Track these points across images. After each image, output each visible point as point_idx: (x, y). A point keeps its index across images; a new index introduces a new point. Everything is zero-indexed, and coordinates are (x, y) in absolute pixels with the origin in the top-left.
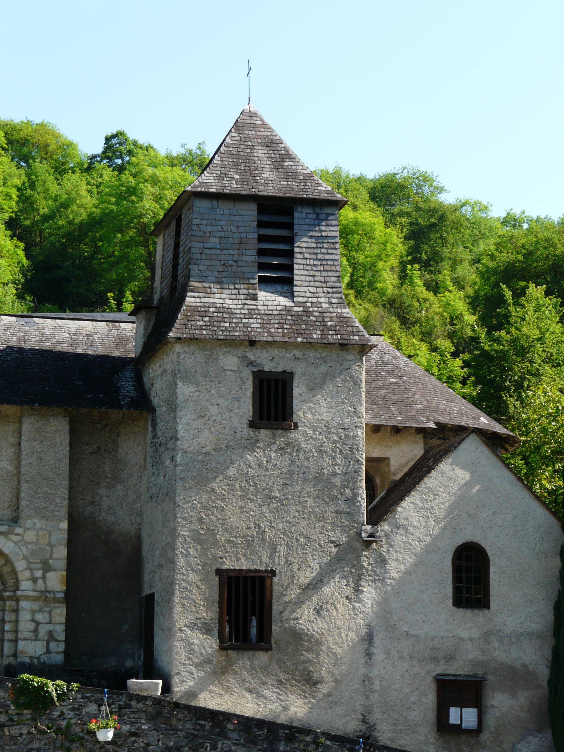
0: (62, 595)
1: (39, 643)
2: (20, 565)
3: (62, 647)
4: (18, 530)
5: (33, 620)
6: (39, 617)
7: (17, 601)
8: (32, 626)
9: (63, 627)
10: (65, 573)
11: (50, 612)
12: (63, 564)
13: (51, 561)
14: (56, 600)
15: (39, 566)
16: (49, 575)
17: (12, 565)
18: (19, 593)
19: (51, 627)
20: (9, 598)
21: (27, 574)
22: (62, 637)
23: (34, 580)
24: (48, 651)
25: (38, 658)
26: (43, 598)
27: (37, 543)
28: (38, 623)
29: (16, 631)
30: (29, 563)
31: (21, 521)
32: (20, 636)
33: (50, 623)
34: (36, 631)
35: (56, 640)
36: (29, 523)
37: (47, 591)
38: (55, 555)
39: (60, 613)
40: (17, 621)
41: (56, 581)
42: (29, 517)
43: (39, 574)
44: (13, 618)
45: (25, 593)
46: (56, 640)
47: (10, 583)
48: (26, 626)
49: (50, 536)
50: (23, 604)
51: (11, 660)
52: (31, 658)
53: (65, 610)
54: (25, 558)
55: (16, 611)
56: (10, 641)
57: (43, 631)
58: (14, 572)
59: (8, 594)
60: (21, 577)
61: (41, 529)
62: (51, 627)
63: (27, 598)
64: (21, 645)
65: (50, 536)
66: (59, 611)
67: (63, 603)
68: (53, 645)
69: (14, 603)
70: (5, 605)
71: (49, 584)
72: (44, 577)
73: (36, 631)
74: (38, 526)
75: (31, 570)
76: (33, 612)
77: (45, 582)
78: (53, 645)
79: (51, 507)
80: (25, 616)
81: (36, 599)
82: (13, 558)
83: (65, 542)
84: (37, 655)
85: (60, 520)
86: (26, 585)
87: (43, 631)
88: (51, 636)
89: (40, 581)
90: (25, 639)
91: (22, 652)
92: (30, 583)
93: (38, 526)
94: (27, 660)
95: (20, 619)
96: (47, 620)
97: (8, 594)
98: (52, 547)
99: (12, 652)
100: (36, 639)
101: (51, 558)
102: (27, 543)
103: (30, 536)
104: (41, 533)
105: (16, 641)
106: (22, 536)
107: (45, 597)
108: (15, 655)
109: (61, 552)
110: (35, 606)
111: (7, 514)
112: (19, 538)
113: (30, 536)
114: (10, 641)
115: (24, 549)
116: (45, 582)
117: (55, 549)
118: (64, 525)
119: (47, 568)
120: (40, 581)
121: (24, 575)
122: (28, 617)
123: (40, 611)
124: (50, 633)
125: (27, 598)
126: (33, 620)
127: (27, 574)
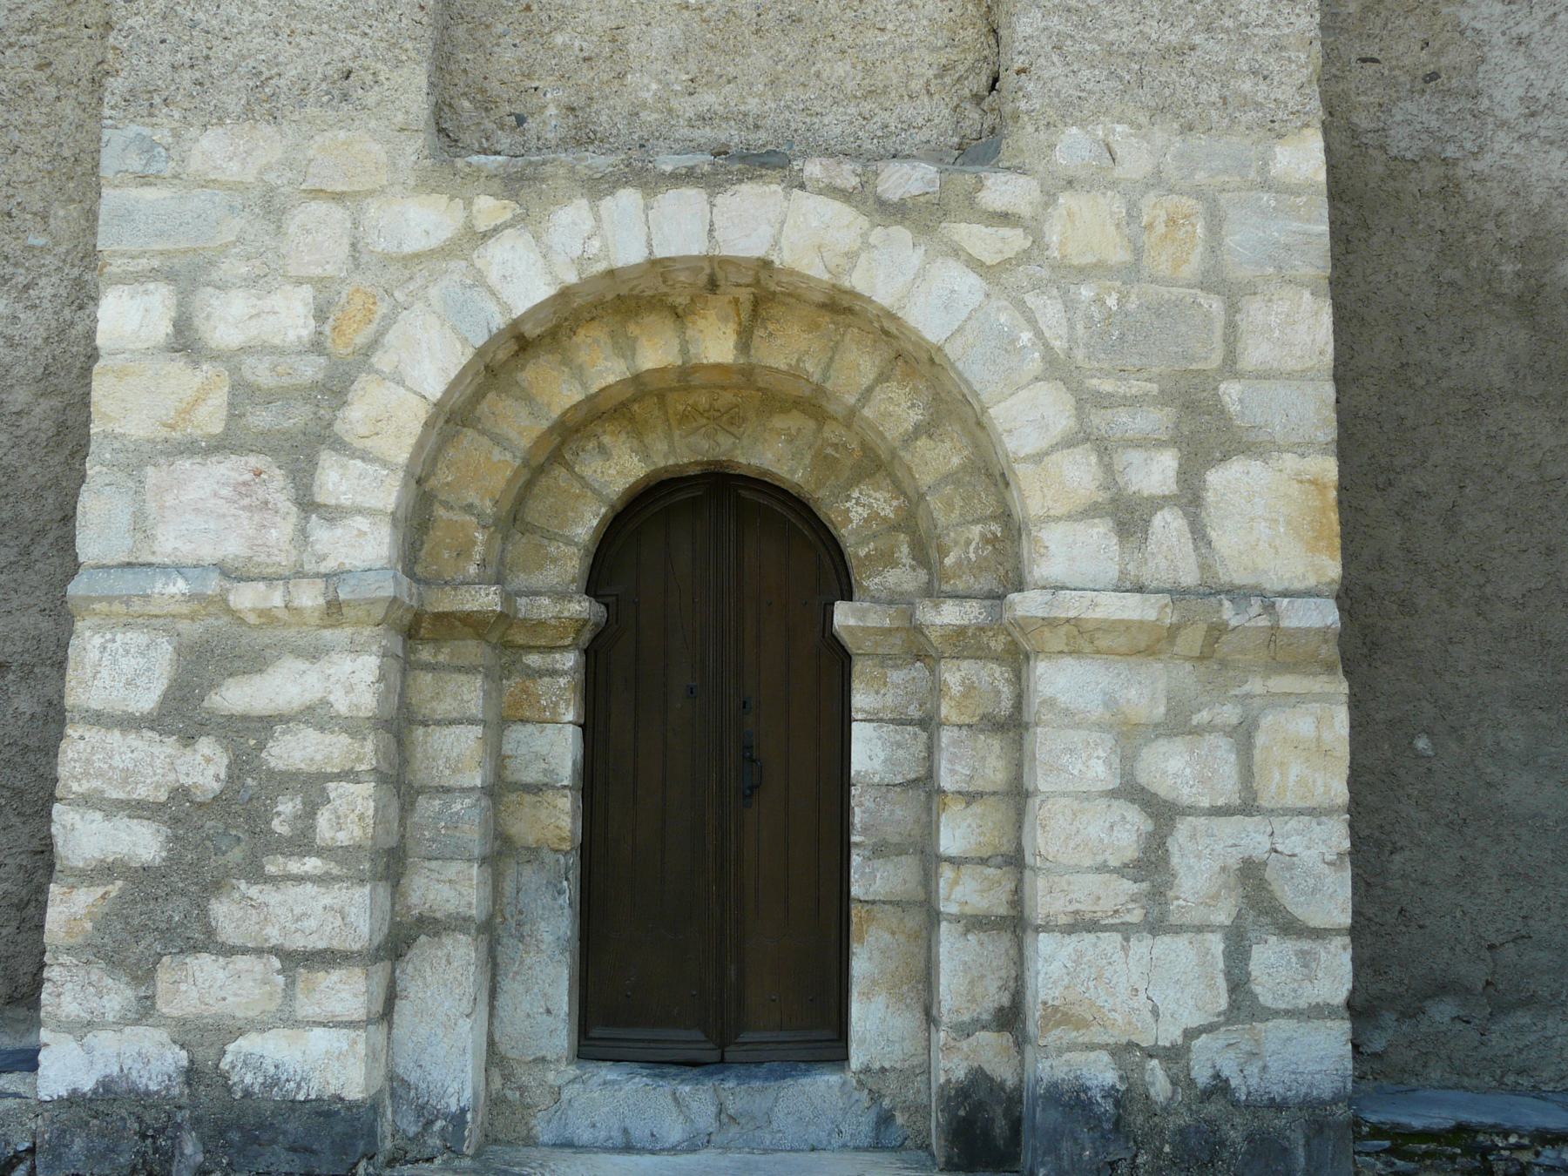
0: (1327, 615)
1: (1177, 951)
2: (1027, 418)
3: (1334, 975)
4: (1001, 190)
5: (1132, 792)
6: (1172, 768)
7: (1017, 659)
8: (1125, 832)
9: (1336, 835)
10: (1328, 468)
11: (1243, 736)
12: (1311, 408)
13: (1231, 391)
14: (1282, 651)
15: (1155, 420)
16: (1228, 481)
17: (977, 426)
18: (1027, 604)
19: (1252, 837)
20: (964, 643)
21: (1079, 474)
22: (1331, 901)
23: (1128, 517)
24: (1242, 1002)
25: (1174, 1055)
26: (1192, 639)
27: (1132, 272)
28: (1163, 813)
29: (1015, 861)
30: (1087, 401)
31: (1024, 137)
32: (1046, 901)
33: (1248, 807)
34: (1151, 865)
35: (1290, 928)
36: (1073, 146)
37: (1212, 590)
38: (1255, 354)
39: (1309, 739)
40: (1018, 795)
41: (1275, 523)
42: (1069, 110)
43: (1156, 473)
44: (995, 772)
45: (1072, 606)
46: (1290, 928)
47: (965, 542)
48: (1081, 835)
49: (1215, 223)
50: (1058, 680)
51: (990, 1053)
52: (1122, 1051)
53: (1341, 719)
54: (1057, 368)
55: (1012, 725)
56: (976, 923)
57: (1200, 864)
58: (990, 474)
59: (950, 614)
60: (1034, 496)
61: (1156, 181)
62: (1252, 837)
63: (1083, 638)
64: (1054, 965)
65: (1215, 223)
66: (1302, 724)
67: (1329, 669)
68: (1271, 961)
69: (994, 676)
70: (937, 689)
71: (1226, 539)
72: (1190, 498)
73: (1151, 865)
74: (1135, 161)
75: (1104, 448)
76: (1129, 736)
77: (1199, 533)
78: (1271, 961)
79: (1214, 50)
80: (1071, 765)
81: (1148, 645)
82: (975, 368)
83: (1315, 261)
84: (1169, 1034)
85: (1275, 130)
86: (1071, 557)
87: (1200, 864)
88: (1258, 899)
89: (1168, 526)
90: (1082, 925)
91: (1058, 1016)
92: (1099, 532)
93: (1135, 161)
94: (1101, 1073)
95: (1043, 782)
96: (1227, 790)
97: (950, 614)
98: (1233, 295)
99: (994, 997)
100: (1156, 926)
101: (1230, 366)
102: (1067, 274)
103: (1086, 227)
104: (1154, 208)
105: (1015, 924)
106: (1034, 228)
107: (1206, 630)
108: (1010, 1018)
109: (1295, 331)
110: (1143, 691)
111: (934, 116)
112: (1016, 240)
113: (1086, 227)
114: (976, 923)
115: (1049, 311)
116: (1199, 533)
117: (1254, 312)
118: (1303, 159)
119: (1206, 436)
120: (1168, 526)
121: (1054, 482)
122: (1098, 769)
123: (1178, 724)
124: (1251, 874)
125: (1083, 638)
126: (1132, 792)
127: (1079, 474)
